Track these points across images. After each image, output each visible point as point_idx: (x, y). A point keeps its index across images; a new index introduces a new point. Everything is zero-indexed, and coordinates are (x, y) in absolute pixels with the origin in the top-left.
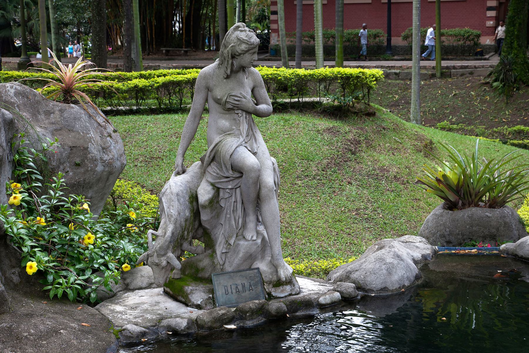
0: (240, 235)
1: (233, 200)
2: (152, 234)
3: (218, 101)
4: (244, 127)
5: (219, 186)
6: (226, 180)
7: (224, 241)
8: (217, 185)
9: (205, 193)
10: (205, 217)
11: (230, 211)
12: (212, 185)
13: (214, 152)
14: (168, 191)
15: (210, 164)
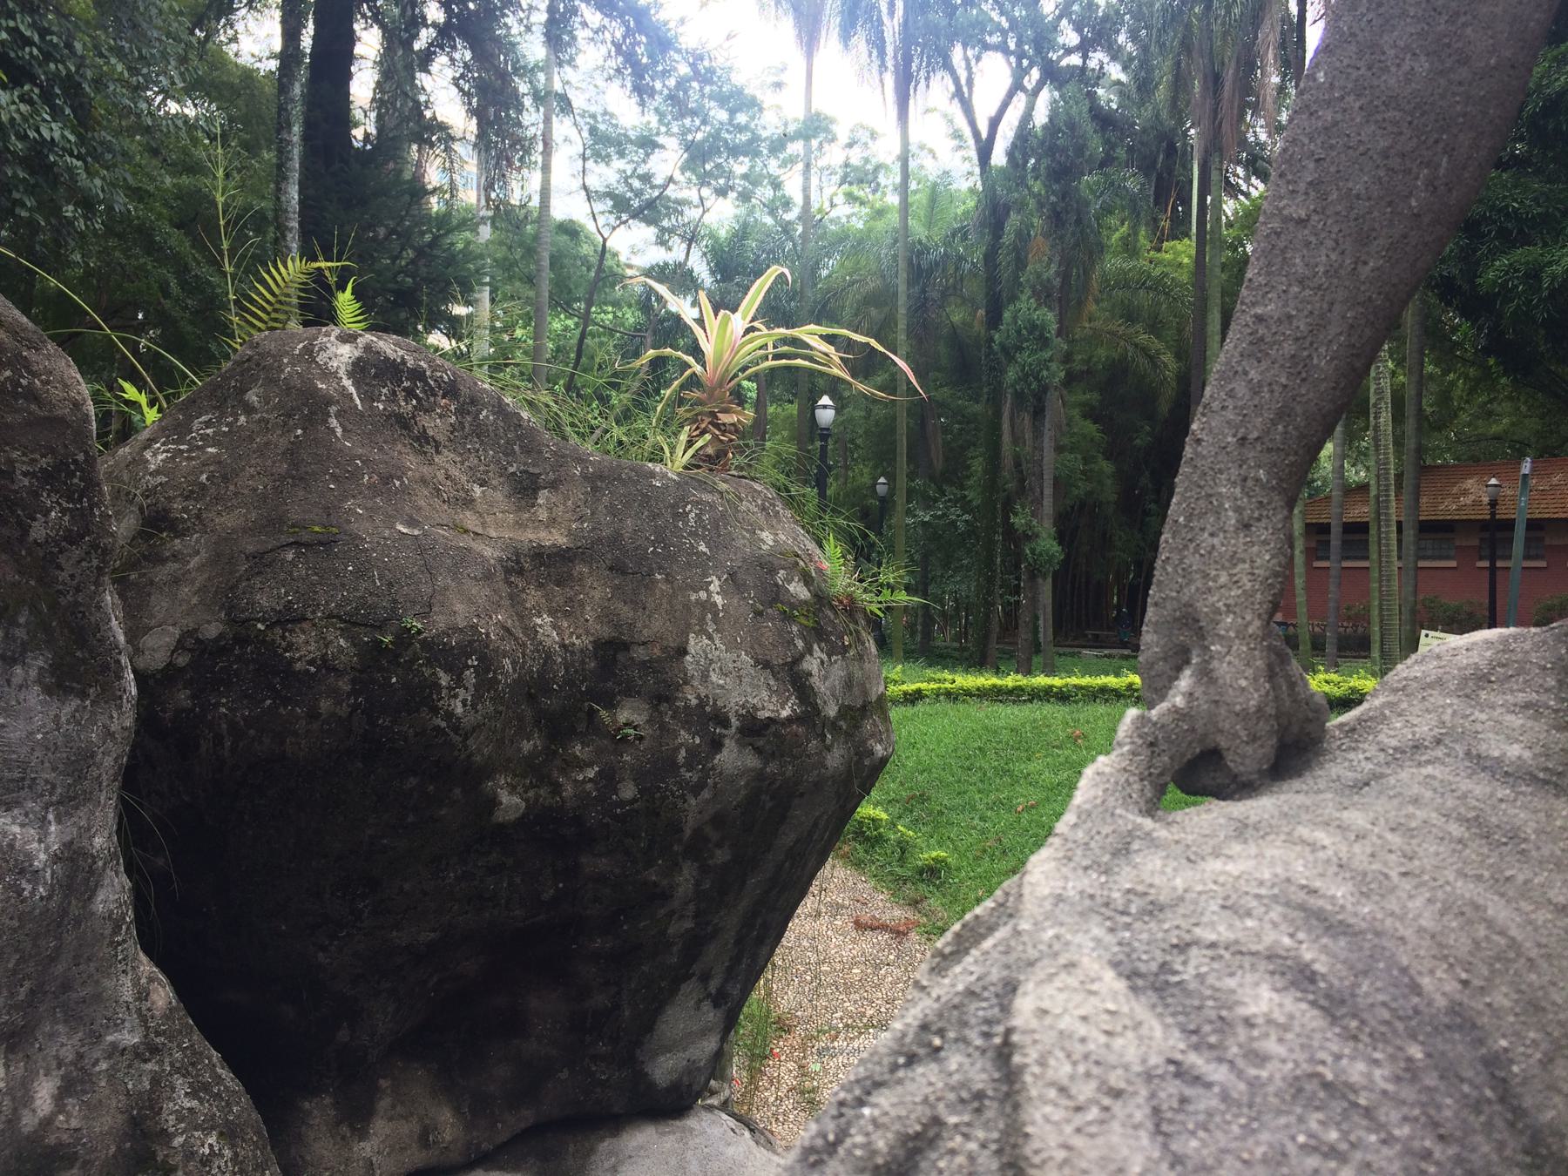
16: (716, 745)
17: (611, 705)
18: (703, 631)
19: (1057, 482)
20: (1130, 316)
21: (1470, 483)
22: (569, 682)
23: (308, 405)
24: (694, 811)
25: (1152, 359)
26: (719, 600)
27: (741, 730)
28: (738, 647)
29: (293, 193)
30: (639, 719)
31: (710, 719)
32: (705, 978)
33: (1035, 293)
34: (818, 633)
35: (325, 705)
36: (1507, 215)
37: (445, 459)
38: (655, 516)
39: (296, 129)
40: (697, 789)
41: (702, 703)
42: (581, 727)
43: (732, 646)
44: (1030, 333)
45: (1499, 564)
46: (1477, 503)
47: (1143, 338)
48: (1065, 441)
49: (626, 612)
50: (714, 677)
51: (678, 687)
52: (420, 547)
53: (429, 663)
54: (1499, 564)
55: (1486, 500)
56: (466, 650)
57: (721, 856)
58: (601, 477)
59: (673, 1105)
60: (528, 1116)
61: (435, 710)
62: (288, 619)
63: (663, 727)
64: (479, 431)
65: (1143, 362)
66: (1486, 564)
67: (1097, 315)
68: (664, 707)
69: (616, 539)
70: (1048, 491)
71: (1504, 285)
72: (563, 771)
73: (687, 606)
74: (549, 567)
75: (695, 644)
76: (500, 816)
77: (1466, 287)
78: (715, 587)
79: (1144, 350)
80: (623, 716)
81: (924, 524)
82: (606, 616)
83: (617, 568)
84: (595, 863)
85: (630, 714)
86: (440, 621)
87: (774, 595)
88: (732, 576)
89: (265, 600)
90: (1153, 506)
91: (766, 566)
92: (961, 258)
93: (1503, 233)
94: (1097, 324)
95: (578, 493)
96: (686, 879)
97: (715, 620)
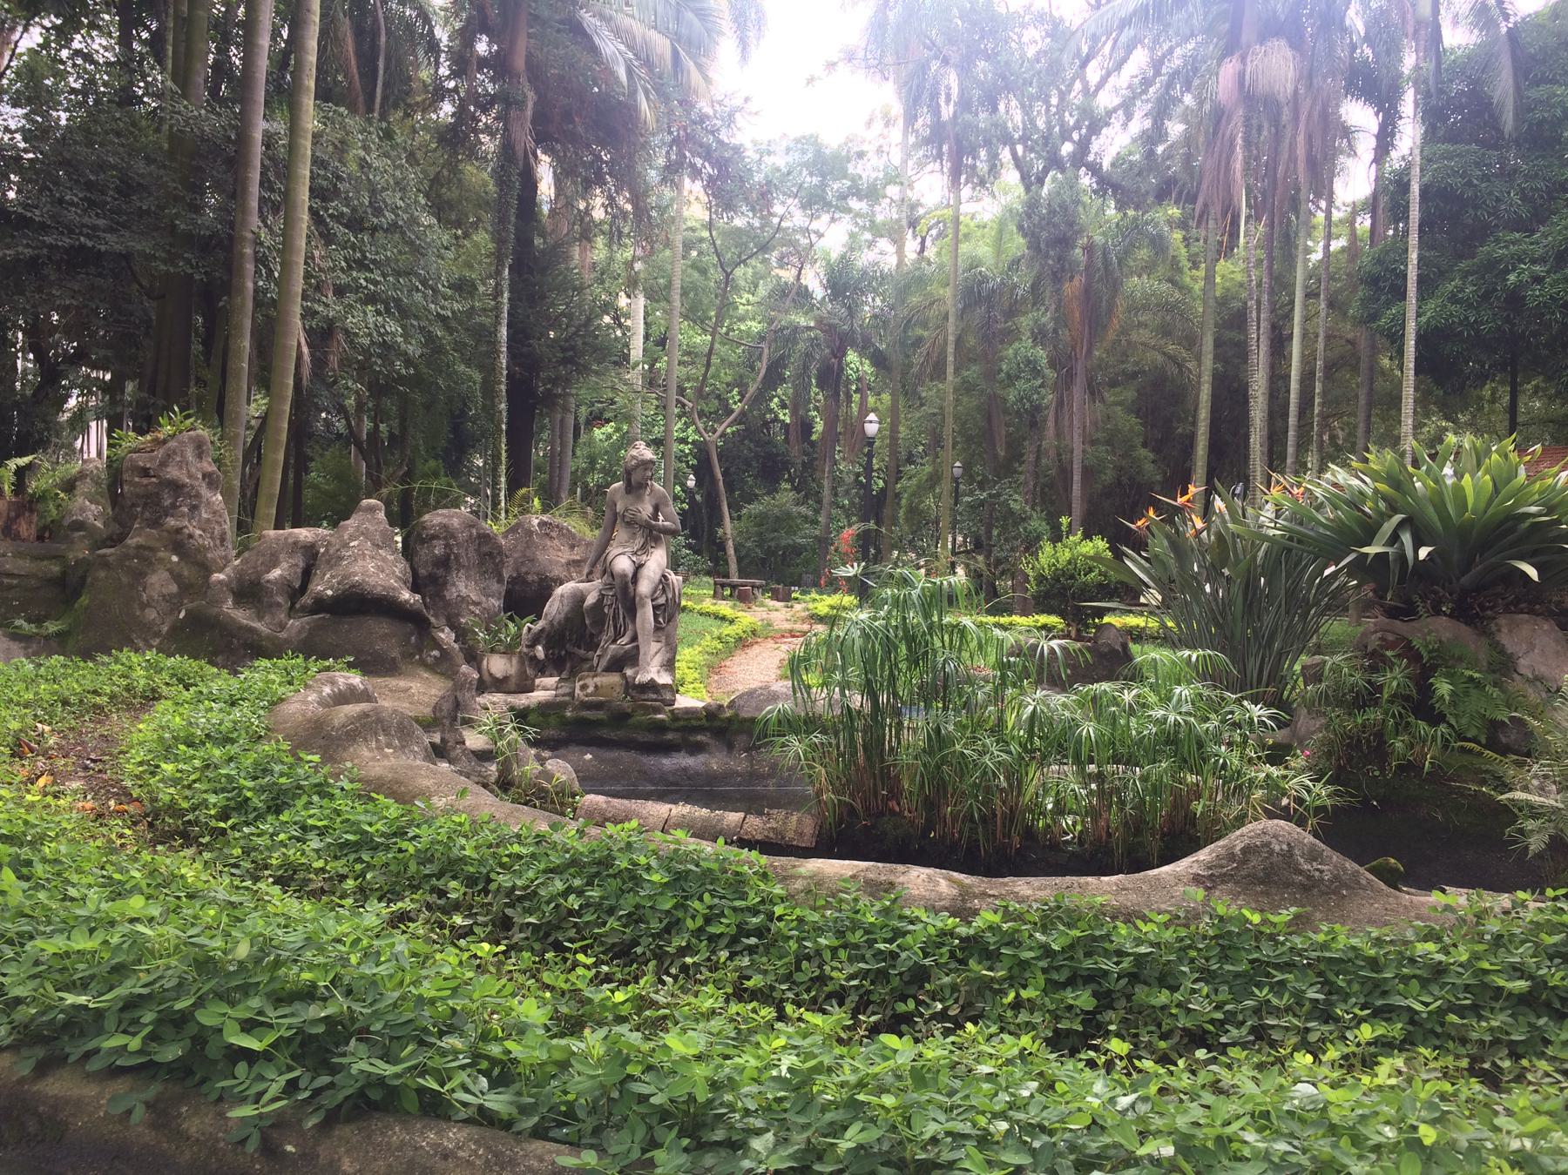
0: (614, 641)
4: (639, 541)
19: (1088, 472)
23: (530, 533)
29: (504, 331)
37: (556, 542)
39: (506, 295)
47: (1171, 348)
48: (1100, 435)
70: (1077, 477)
89: (524, 570)
92: (1015, 286)
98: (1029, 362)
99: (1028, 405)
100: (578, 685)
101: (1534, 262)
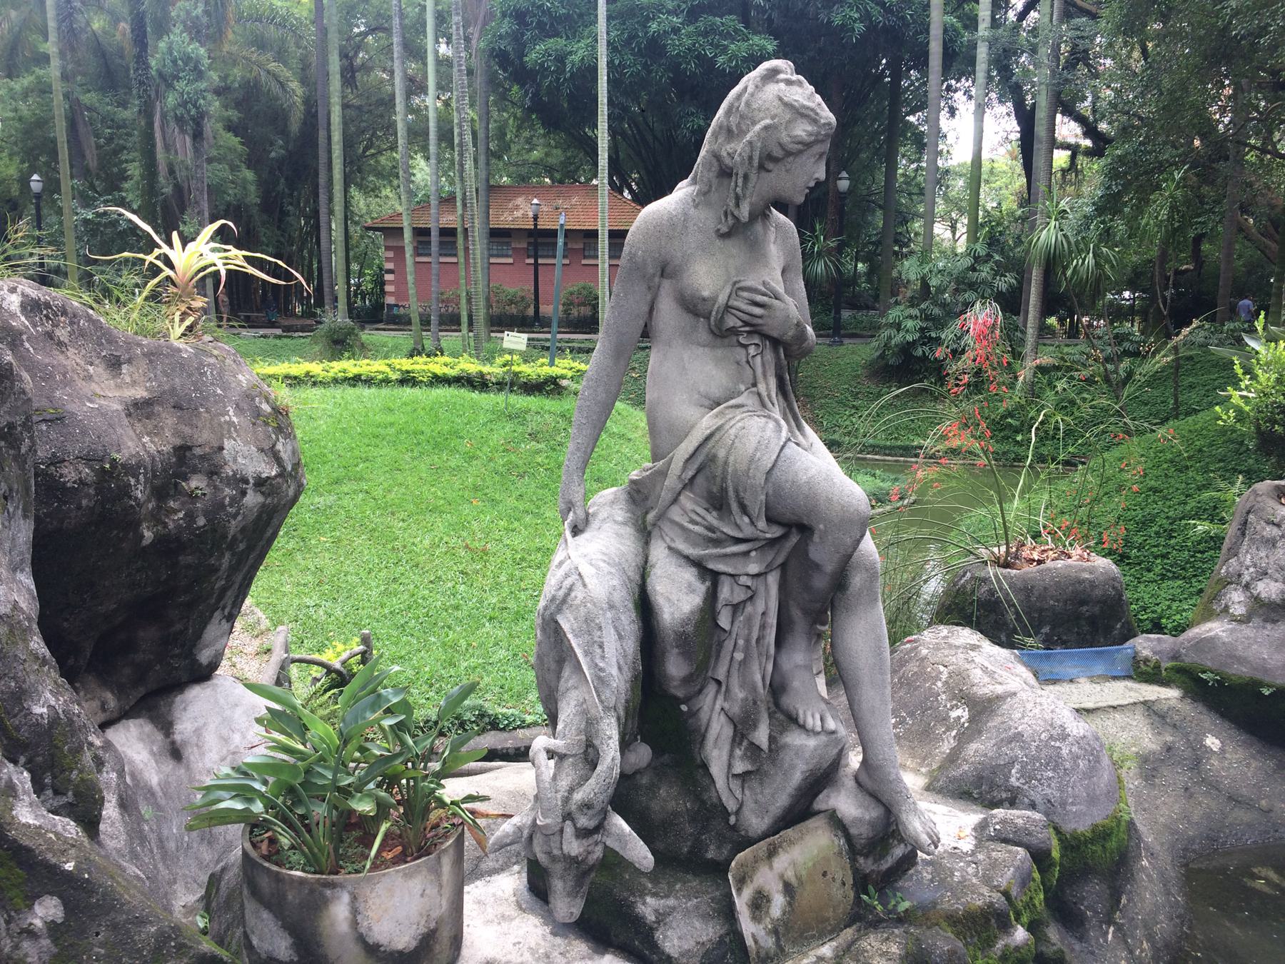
1: (761, 609)
2: (548, 751)
3: (693, 307)
5: (721, 567)
6: (742, 548)
7: (728, 731)
8: (711, 566)
9: (677, 596)
10: (675, 667)
11: (747, 641)
12: (698, 564)
13: (700, 458)
14: (579, 594)
15: (675, 500)
16: (244, 493)
17: (186, 479)
18: (231, 437)
20: (261, 44)
21: (520, 201)
22: (164, 470)
24: (234, 526)
25: (282, 85)
26: (235, 419)
27: (255, 485)
28: (249, 443)
30: (202, 485)
31: (239, 481)
32: (223, 609)
33: (186, 29)
34: (279, 430)
35: (84, 502)
36: (543, 12)
37: (71, 352)
38: (190, 376)
40: (235, 516)
41: (235, 474)
42: (172, 492)
43: (246, 443)
44: (186, 64)
45: (540, 261)
46: (525, 216)
47: (272, 66)
49: (187, 430)
50: (240, 460)
51: (222, 467)
52: (101, 412)
53: (126, 474)
54: (540, 261)
55: (531, 214)
56: (139, 465)
57: (242, 546)
58: (152, 354)
59: (204, 674)
60: (142, 691)
61: (130, 497)
62: (56, 461)
63: (215, 487)
64: (82, 334)
65: (276, 89)
66: (532, 261)
67: (233, 41)
68: (215, 477)
69: (173, 390)
71: (542, 65)
72: (167, 516)
73: (220, 425)
74: (140, 410)
75: (228, 444)
76: (145, 542)
77: (517, 62)
78: (231, 413)
79: (276, 77)
80: (193, 484)
81: (86, 221)
82: (177, 433)
83: (177, 407)
84: (187, 559)
85: (196, 483)
86: (126, 453)
87: (257, 413)
88: (237, 405)
90: (290, 208)
91: (249, 396)
93: (541, 25)
94: (234, 49)
95: (143, 364)
96: (226, 560)
97: (236, 431)
98: (189, 58)
99: (193, 112)
100: (741, 903)
101: (669, 12)
